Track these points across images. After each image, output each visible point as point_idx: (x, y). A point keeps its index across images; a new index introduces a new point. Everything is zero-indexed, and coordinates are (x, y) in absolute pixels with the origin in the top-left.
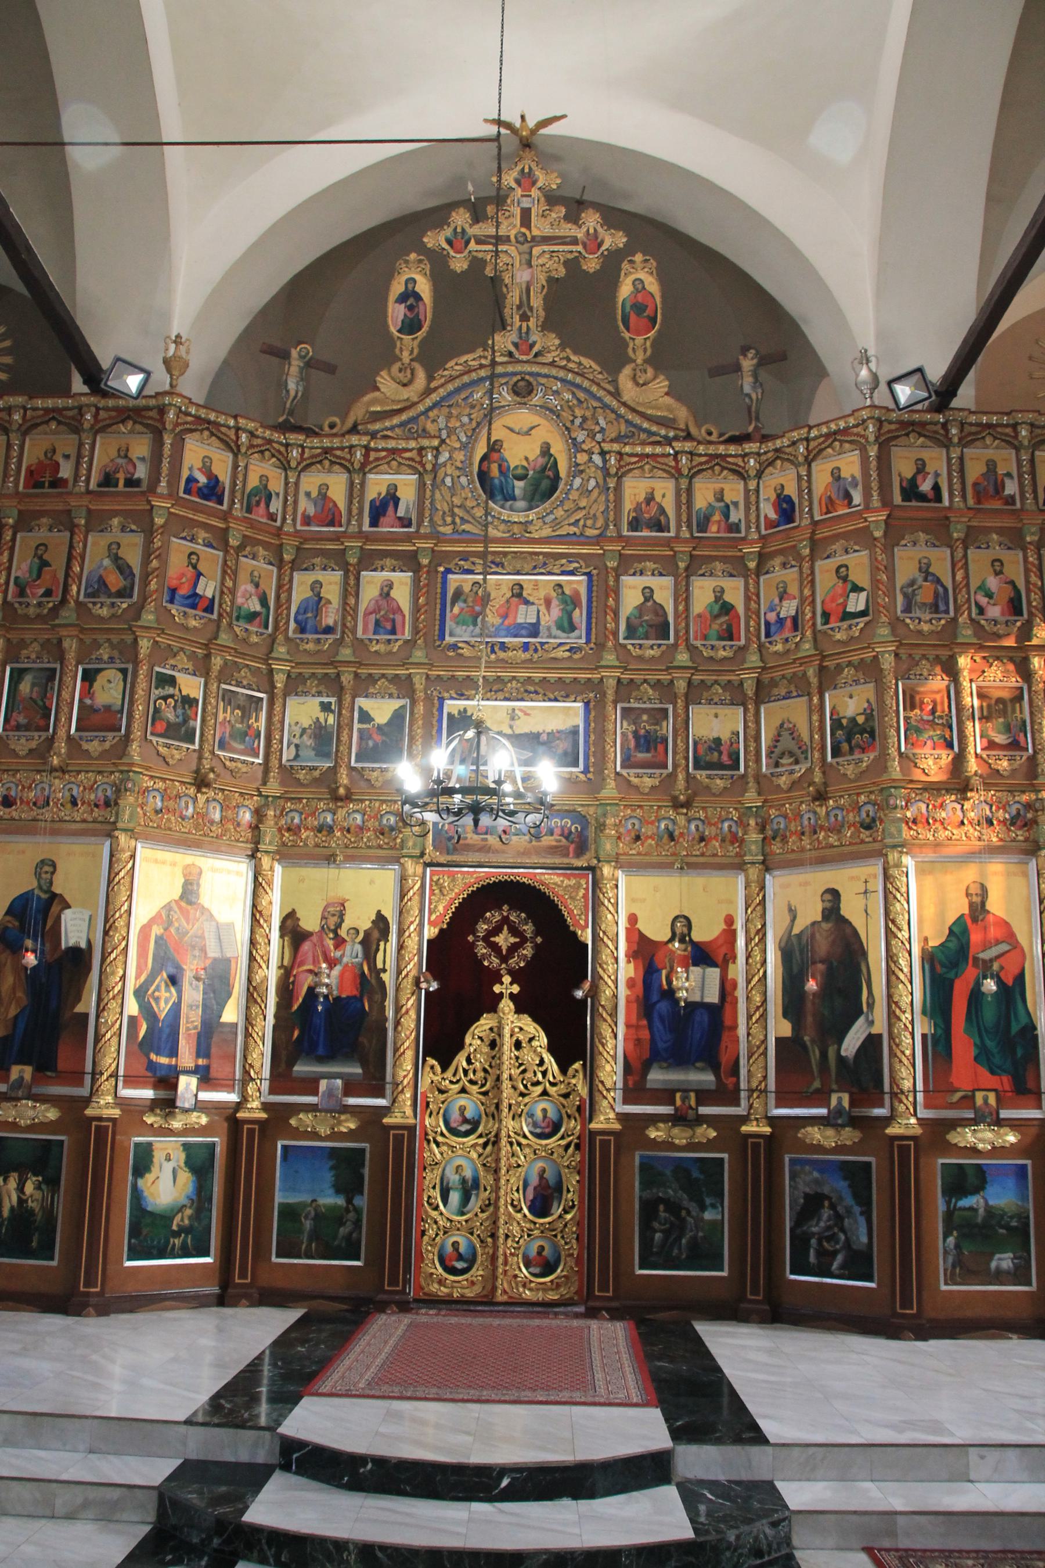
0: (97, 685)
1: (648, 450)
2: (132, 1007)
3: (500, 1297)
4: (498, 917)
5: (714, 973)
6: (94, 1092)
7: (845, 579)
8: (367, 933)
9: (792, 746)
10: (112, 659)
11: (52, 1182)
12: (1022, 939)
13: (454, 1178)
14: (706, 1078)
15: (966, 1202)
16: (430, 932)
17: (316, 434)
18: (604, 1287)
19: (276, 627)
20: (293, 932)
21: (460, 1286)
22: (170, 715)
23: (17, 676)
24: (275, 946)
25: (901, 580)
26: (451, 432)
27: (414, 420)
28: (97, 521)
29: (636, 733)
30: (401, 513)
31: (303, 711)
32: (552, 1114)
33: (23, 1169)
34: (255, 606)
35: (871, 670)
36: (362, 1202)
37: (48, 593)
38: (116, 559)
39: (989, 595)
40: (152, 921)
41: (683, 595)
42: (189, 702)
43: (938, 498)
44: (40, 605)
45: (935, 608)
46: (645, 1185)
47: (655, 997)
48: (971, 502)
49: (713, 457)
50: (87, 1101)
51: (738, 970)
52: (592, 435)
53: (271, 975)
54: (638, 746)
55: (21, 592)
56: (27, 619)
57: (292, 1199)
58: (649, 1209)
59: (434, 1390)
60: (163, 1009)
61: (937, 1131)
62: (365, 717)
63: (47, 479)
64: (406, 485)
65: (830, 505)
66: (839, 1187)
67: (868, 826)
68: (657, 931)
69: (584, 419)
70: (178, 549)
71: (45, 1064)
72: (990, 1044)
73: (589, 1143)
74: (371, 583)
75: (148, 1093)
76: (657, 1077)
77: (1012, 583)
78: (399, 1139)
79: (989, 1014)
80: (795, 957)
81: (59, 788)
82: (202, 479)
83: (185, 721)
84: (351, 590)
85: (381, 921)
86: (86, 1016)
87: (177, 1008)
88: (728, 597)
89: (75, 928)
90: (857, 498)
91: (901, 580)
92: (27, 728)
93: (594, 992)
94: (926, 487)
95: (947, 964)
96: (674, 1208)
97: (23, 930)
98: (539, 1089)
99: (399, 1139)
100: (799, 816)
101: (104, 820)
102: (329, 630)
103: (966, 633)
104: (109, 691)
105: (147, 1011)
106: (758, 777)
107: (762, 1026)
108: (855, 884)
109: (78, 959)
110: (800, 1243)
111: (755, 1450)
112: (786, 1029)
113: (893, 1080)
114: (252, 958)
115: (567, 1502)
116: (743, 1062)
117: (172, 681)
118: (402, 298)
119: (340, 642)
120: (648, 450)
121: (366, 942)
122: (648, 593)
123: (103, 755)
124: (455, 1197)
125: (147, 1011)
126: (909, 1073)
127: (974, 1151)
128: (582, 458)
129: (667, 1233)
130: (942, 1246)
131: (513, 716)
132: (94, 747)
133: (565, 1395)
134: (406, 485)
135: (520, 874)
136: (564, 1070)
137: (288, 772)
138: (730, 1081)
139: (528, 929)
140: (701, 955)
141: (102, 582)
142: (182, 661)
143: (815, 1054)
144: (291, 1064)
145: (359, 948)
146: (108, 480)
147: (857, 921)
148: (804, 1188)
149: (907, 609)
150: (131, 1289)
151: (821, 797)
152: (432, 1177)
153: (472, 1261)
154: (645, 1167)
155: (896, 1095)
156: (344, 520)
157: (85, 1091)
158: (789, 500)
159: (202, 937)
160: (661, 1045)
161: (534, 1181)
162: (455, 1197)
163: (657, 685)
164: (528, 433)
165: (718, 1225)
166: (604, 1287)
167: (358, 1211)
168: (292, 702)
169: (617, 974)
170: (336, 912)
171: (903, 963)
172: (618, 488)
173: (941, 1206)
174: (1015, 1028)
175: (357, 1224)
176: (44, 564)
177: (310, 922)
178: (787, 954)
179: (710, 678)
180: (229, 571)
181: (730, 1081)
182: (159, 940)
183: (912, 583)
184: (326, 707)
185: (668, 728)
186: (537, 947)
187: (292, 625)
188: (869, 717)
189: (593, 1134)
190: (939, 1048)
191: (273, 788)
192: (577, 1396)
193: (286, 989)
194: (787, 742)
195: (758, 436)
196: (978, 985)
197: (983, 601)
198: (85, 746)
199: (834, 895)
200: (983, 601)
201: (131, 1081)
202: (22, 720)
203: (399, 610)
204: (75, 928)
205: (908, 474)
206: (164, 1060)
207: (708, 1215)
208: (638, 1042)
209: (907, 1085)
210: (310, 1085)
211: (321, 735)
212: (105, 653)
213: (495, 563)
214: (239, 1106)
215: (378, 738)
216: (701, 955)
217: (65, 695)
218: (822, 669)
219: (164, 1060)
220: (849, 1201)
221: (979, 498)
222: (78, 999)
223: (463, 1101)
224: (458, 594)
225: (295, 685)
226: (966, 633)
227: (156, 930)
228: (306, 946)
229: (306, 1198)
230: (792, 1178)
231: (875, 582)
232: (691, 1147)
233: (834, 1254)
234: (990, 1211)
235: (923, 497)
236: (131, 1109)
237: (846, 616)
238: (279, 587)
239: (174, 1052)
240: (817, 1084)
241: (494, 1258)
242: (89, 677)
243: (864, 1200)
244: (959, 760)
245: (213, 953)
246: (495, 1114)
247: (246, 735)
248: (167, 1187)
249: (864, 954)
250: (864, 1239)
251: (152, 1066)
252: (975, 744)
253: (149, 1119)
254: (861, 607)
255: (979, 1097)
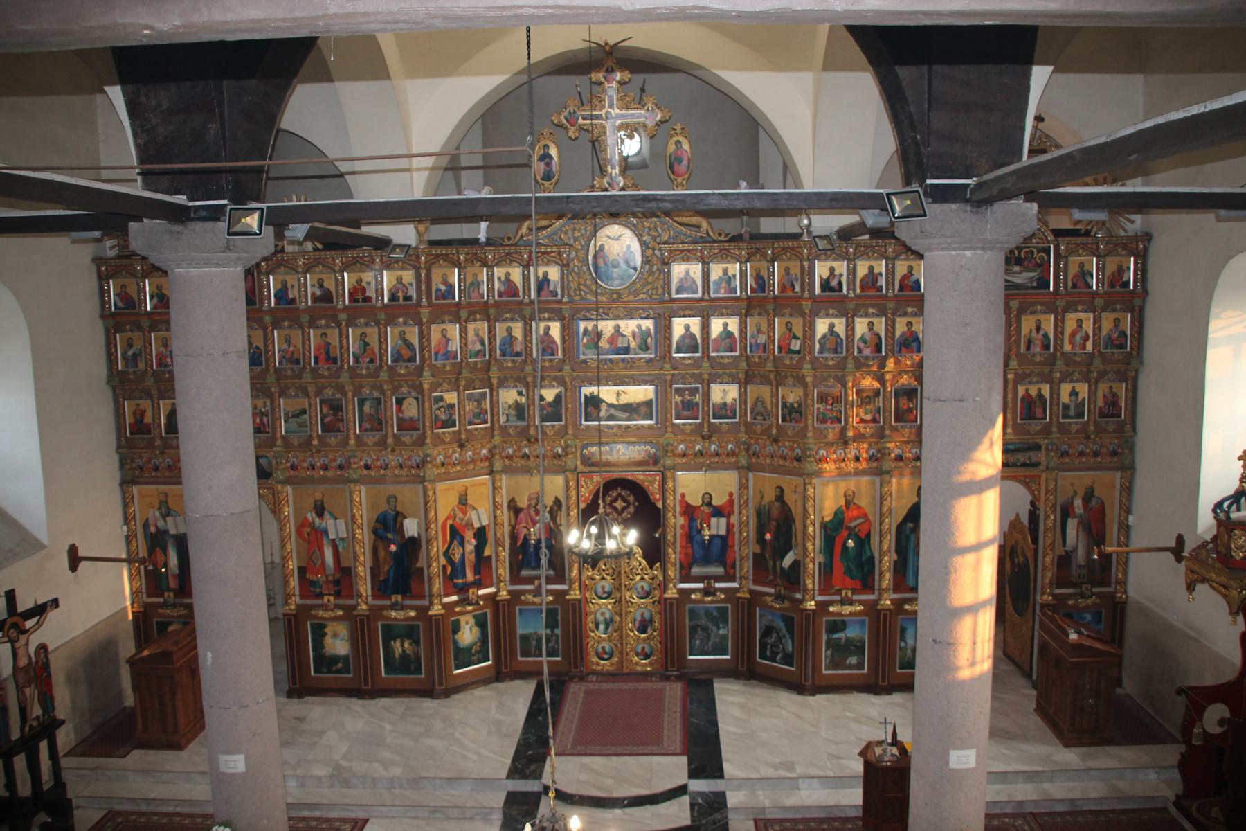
0: (404, 407)
1: (686, 247)
2: (443, 561)
3: (625, 671)
4: (615, 494)
5: (723, 520)
6: (431, 604)
7: (790, 330)
8: (551, 508)
9: (762, 410)
10: (410, 393)
11: (417, 642)
12: (870, 517)
13: (600, 618)
14: (720, 570)
15: (836, 636)
16: (583, 506)
17: (502, 245)
18: (673, 666)
19: (490, 355)
20: (515, 509)
21: (605, 665)
22: (443, 417)
23: (362, 402)
24: (505, 516)
25: (818, 335)
26: (576, 239)
27: (555, 233)
28: (391, 321)
29: (682, 402)
30: (551, 288)
31: (509, 396)
32: (647, 588)
33: (402, 637)
34: (478, 347)
35: (801, 381)
36: (558, 631)
37: (372, 361)
38: (405, 341)
39: (865, 342)
40: (448, 518)
41: (705, 327)
42: (451, 406)
43: (841, 289)
44: (368, 368)
45: (836, 351)
46: (691, 619)
47: (694, 533)
48: (858, 291)
49: (721, 250)
50: (428, 609)
51: (734, 519)
52: (654, 238)
53: (507, 530)
54: (683, 407)
55: (357, 360)
56: (362, 376)
57: (526, 632)
58: (693, 629)
59: (598, 748)
60: (457, 558)
61: (822, 606)
62: (542, 398)
63: (360, 297)
64: (554, 273)
65: (783, 288)
66: (781, 625)
67: (798, 459)
68: (695, 500)
69: (650, 229)
70: (435, 332)
71: (406, 591)
72: (851, 565)
73: (662, 601)
74: (539, 327)
75: (455, 598)
76: (696, 570)
77: (878, 335)
78: (574, 605)
79: (852, 554)
80: (762, 516)
81: (393, 460)
82: (443, 288)
83: (451, 415)
84: (527, 332)
85: (557, 501)
86: (422, 569)
87: (463, 555)
88: (729, 328)
89: (411, 527)
90: (797, 288)
91: (818, 335)
92: (371, 430)
93: (664, 534)
94: (834, 283)
95: (833, 530)
96: (705, 629)
97: (387, 529)
98: (638, 578)
99: (574, 605)
100: (764, 447)
101: (417, 473)
102: (518, 354)
103: (850, 365)
104: (410, 409)
105: (450, 561)
106: (746, 424)
107: (745, 551)
108: (789, 483)
109: (414, 543)
110: (763, 646)
111: (719, 781)
112: (758, 550)
113: (805, 585)
114: (496, 524)
115: (649, 807)
116: (737, 563)
117: (441, 399)
118: (541, 159)
119: (525, 362)
120: (686, 247)
121: (551, 512)
122: (687, 328)
123: (414, 444)
124: (602, 627)
125: (450, 561)
126: (811, 582)
127: (840, 614)
128: (649, 252)
129: (702, 641)
130: (825, 654)
131: (618, 394)
132: (407, 439)
133: (651, 748)
134: (554, 273)
135: (629, 476)
136: (651, 568)
137: (504, 430)
138: (731, 571)
139: (631, 499)
140: (718, 512)
141: (398, 352)
142: (446, 386)
143: (771, 563)
144: (519, 570)
145: (547, 515)
146: (393, 297)
147: (792, 506)
148: (765, 623)
149: (821, 352)
150: (459, 682)
151: (776, 440)
152: (591, 618)
153: (611, 655)
154: (691, 611)
155: (805, 590)
156: (521, 293)
157: (426, 603)
158: (762, 279)
159: (470, 519)
160: (697, 556)
161: (639, 618)
162: (602, 627)
163: (693, 376)
164: (618, 239)
165: (724, 637)
166: (673, 666)
167: (557, 636)
168: (502, 392)
169: (676, 522)
170: (537, 499)
171: (811, 529)
172: (669, 272)
173: (824, 637)
174: (864, 558)
175: (557, 641)
176: (367, 344)
177: (523, 502)
178: (759, 514)
179: (721, 371)
180: (463, 332)
181: (731, 571)
182: (452, 526)
183: (824, 337)
184: (520, 393)
185: (698, 398)
186: (636, 507)
187: (498, 352)
188: (800, 405)
189: (666, 599)
190: (827, 571)
191: (497, 439)
192: (655, 749)
193: (513, 537)
194: (759, 408)
195: (746, 237)
196: (845, 543)
197: (862, 345)
198: (403, 439)
199: (782, 490)
200: (862, 345)
201: (447, 595)
202: (368, 426)
203: (554, 342)
204: (411, 527)
205: (826, 274)
206: (460, 581)
207: (721, 632)
208: (686, 554)
209: (810, 586)
210: (530, 580)
211: (519, 411)
212: (405, 390)
213: (606, 316)
214: (496, 594)
215: (550, 409)
216: (718, 512)
217: (389, 413)
218: (778, 373)
219: (460, 581)
220: (784, 630)
221: (862, 289)
222: (417, 560)
223: (603, 583)
224: (586, 331)
225: (502, 383)
226: (850, 365)
227: (450, 522)
228: (522, 515)
229: (532, 631)
230: (761, 616)
231: (805, 337)
232: (712, 602)
233: (777, 653)
234: (848, 640)
235: (832, 289)
236: (449, 607)
237: (790, 351)
238: (490, 332)
239: (464, 576)
240: (771, 577)
241: (621, 653)
242: (399, 402)
243: (791, 631)
244: (844, 430)
245: (477, 525)
246: (618, 589)
247: (480, 416)
248: (468, 635)
249: (794, 521)
250: (790, 649)
251: (455, 585)
252: (854, 421)
253: (457, 609)
254: (797, 348)
255: (843, 593)
